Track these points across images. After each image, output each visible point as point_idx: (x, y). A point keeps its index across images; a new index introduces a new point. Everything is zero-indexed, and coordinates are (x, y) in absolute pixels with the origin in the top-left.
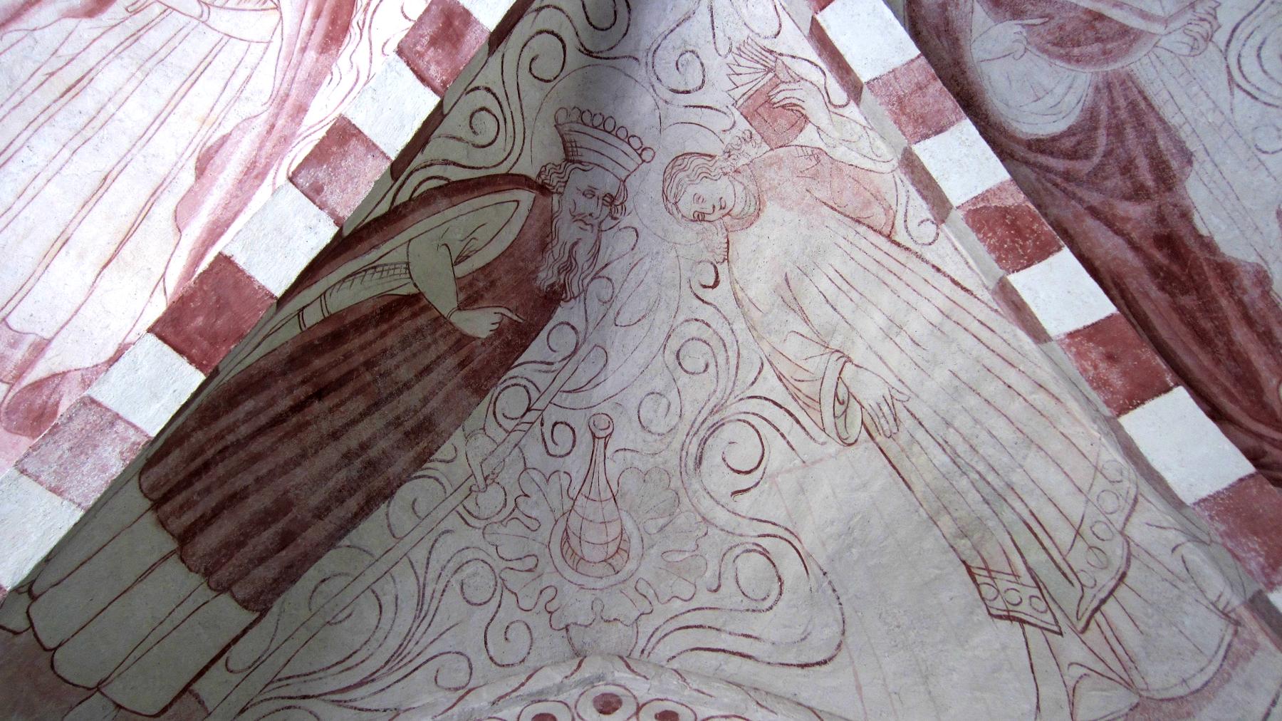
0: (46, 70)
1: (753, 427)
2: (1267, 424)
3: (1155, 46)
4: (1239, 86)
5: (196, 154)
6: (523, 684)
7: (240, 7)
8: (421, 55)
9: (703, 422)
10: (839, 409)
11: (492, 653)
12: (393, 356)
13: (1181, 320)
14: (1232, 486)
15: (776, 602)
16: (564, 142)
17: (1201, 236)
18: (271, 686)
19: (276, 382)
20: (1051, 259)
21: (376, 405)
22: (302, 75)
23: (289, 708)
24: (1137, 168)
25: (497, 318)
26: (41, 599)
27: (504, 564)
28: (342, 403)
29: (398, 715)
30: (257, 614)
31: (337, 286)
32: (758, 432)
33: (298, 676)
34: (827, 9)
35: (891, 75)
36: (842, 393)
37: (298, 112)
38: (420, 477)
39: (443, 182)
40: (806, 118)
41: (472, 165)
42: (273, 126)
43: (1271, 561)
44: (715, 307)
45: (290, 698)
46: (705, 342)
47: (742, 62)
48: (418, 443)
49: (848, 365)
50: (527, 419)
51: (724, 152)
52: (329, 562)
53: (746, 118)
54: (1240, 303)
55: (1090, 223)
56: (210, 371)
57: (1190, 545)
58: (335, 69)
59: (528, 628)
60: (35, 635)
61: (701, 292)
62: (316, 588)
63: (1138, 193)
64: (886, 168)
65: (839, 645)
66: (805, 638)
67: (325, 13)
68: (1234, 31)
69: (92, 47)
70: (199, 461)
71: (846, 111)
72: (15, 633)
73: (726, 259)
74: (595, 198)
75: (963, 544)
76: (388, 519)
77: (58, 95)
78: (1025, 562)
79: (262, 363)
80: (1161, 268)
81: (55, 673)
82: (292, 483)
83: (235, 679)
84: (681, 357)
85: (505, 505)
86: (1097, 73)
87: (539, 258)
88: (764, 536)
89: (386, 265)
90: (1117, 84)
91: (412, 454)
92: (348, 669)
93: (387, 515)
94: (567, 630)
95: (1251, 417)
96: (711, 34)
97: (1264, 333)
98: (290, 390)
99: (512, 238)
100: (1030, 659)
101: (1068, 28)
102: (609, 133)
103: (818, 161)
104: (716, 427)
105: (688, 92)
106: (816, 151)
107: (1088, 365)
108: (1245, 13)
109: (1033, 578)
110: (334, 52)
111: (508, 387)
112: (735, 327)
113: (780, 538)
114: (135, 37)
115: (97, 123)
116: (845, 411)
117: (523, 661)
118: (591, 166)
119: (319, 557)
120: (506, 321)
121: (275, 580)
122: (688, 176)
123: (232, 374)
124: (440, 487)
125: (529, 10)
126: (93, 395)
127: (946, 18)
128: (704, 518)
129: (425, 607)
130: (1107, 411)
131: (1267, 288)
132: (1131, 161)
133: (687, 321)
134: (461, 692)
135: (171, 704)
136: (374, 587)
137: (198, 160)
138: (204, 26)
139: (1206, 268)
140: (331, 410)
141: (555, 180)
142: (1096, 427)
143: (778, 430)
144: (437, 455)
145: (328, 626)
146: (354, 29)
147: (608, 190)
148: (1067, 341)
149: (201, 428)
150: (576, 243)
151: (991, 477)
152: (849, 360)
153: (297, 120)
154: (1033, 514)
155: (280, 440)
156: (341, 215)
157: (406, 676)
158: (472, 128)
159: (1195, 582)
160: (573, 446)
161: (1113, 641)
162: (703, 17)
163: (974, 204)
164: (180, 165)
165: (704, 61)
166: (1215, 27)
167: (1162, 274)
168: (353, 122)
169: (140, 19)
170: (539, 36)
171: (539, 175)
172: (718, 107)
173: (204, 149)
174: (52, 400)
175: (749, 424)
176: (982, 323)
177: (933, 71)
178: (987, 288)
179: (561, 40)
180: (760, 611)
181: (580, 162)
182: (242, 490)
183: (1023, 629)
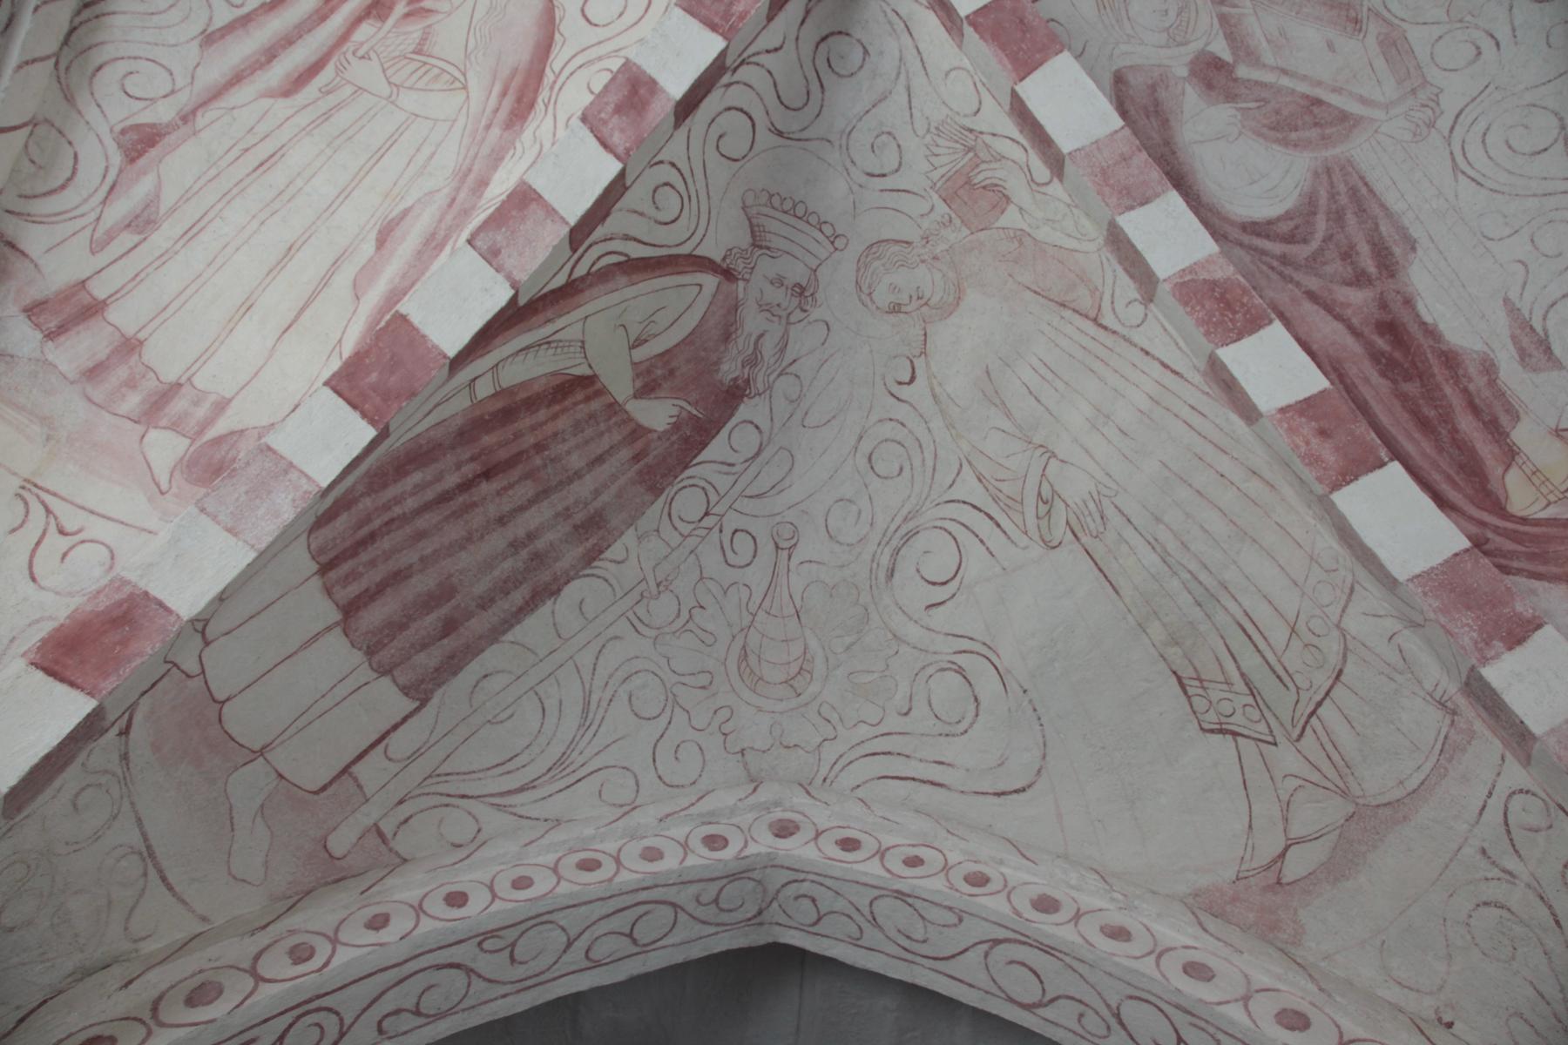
0: (243, 145)
1: (950, 533)
2: (1490, 512)
3: (1376, 131)
4: (1463, 173)
5: (378, 227)
6: (693, 804)
8: (605, 122)
9: (896, 531)
10: (1043, 509)
11: (660, 772)
12: (564, 440)
13: (1403, 407)
14: (1446, 561)
15: (972, 725)
16: (751, 226)
17: (1424, 324)
18: (430, 781)
19: (444, 455)
20: (1262, 332)
21: (545, 493)
22: (485, 150)
23: (447, 805)
24: (1357, 254)
25: (675, 411)
26: (212, 646)
27: (676, 678)
28: (511, 486)
29: (559, 824)
30: (417, 704)
31: (510, 360)
32: (955, 539)
33: (458, 774)
34: (1027, 79)
35: (1094, 146)
36: (1046, 492)
38: (588, 575)
39: (622, 259)
40: (1008, 199)
41: (653, 242)
42: (453, 200)
43: (1485, 636)
44: (911, 405)
45: (449, 795)
46: (899, 443)
47: (940, 141)
48: (587, 539)
49: (1052, 460)
50: (704, 523)
51: (923, 238)
52: (492, 657)
53: (944, 200)
54: (1465, 391)
55: (1308, 307)
56: (382, 427)
57: (1406, 632)
58: (518, 145)
59: (700, 749)
60: (206, 682)
61: (895, 389)
62: (478, 682)
63: (1360, 279)
64: (1092, 247)
65: (1039, 771)
66: (1003, 763)
67: (511, 91)
68: (1457, 117)
70: (365, 531)
71: (1049, 189)
72: (188, 676)
73: (924, 353)
74: (783, 288)
75: (1174, 653)
76: (554, 617)
77: (251, 169)
78: (1239, 668)
79: (432, 433)
80: (1383, 354)
81: (223, 728)
82: (456, 567)
83: (394, 768)
84: (873, 461)
85: (678, 616)
86: (1316, 158)
87: (722, 349)
88: (960, 652)
89: (561, 341)
90: (1337, 169)
91: (581, 550)
92: (509, 772)
93: (553, 612)
94: (743, 755)
95: (1474, 504)
96: (908, 114)
97: (1491, 421)
98: (458, 466)
99: (694, 324)
100: (1243, 774)
101: (1285, 112)
102: (800, 218)
103: (1021, 242)
104: (910, 536)
105: (884, 175)
106: (1018, 233)
107: (1299, 441)
108: (1468, 99)
109: (1247, 684)
110: (517, 128)
111: (685, 487)
112: (931, 425)
113: (978, 653)
114: (326, 116)
115: (286, 196)
116: (1049, 511)
117: (694, 783)
118: (780, 253)
119: (483, 651)
120: (684, 414)
121: (437, 670)
122: (883, 265)
123: (401, 441)
124: (610, 589)
125: (718, 85)
126: (269, 443)
127: (1156, 100)
128: (895, 636)
129: (591, 715)
130: (1319, 489)
131: (1493, 377)
132: (1352, 247)
133: (880, 421)
134: (626, 809)
135: (331, 783)
136: (537, 689)
137: (380, 232)
138: (393, 107)
139: (1429, 356)
140: (498, 493)
141: (740, 266)
142: (1311, 512)
143: (977, 536)
144: (608, 554)
145: (488, 725)
146: (540, 106)
147: (798, 280)
148: (1279, 416)
149: (369, 495)
150: (761, 336)
151: (1203, 576)
152: (1054, 455)
154: (1247, 614)
155: (447, 519)
156: (517, 278)
157: (568, 787)
158: (654, 203)
159: (1412, 673)
160: (754, 557)
161: (1329, 747)
162: (900, 97)
163: (1181, 277)
165: (901, 143)
166: (1438, 111)
167: (1384, 361)
168: (534, 186)
169: (332, 100)
170: (727, 113)
171: (724, 259)
172: (915, 190)
174: (230, 456)
175: (946, 530)
176: (1193, 408)
177: (1137, 142)
178: (1198, 371)
179: (750, 118)
180: (953, 735)
181: (768, 248)
182: (406, 569)
183: (1236, 742)
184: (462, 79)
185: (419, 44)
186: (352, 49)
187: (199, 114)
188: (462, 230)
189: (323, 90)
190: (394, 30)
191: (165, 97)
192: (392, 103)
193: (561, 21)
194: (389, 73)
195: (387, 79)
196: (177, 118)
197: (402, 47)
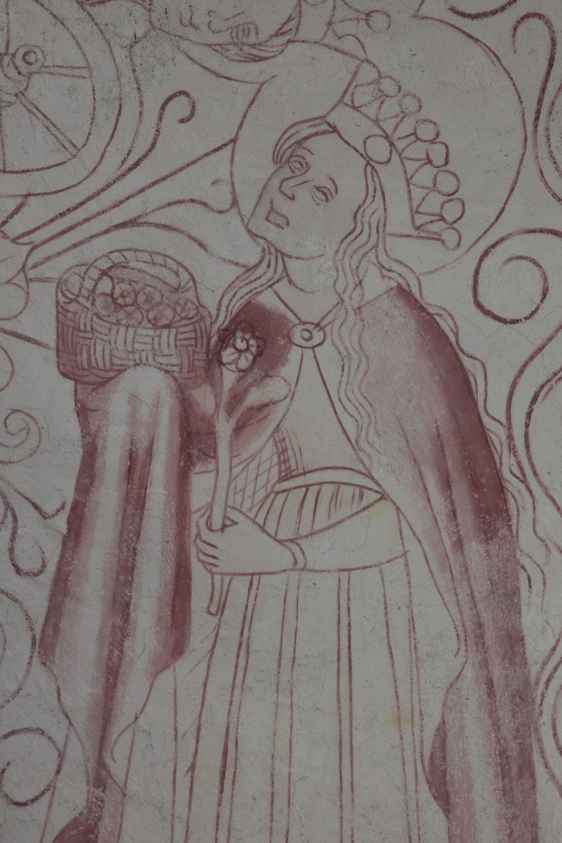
0: (184, 765)
5: (422, 778)
7: (332, 522)
37: (512, 647)
42: (490, 683)
58: (524, 561)
67: (454, 476)
69: (208, 697)
77: (217, 791)
115: (281, 801)
138: (309, 575)
153: (518, 659)
164: (412, 804)
173: (427, 762)
184: (372, 485)
185: (280, 463)
186: (203, 521)
187: (108, 760)
188: (537, 730)
189: (213, 610)
190: (236, 461)
191: (58, 772)
192: (303, 570)
193: (456, 335)
194: (271, 527)
195: (275, 539)
196: (92, 789)
197: (262, 480)
